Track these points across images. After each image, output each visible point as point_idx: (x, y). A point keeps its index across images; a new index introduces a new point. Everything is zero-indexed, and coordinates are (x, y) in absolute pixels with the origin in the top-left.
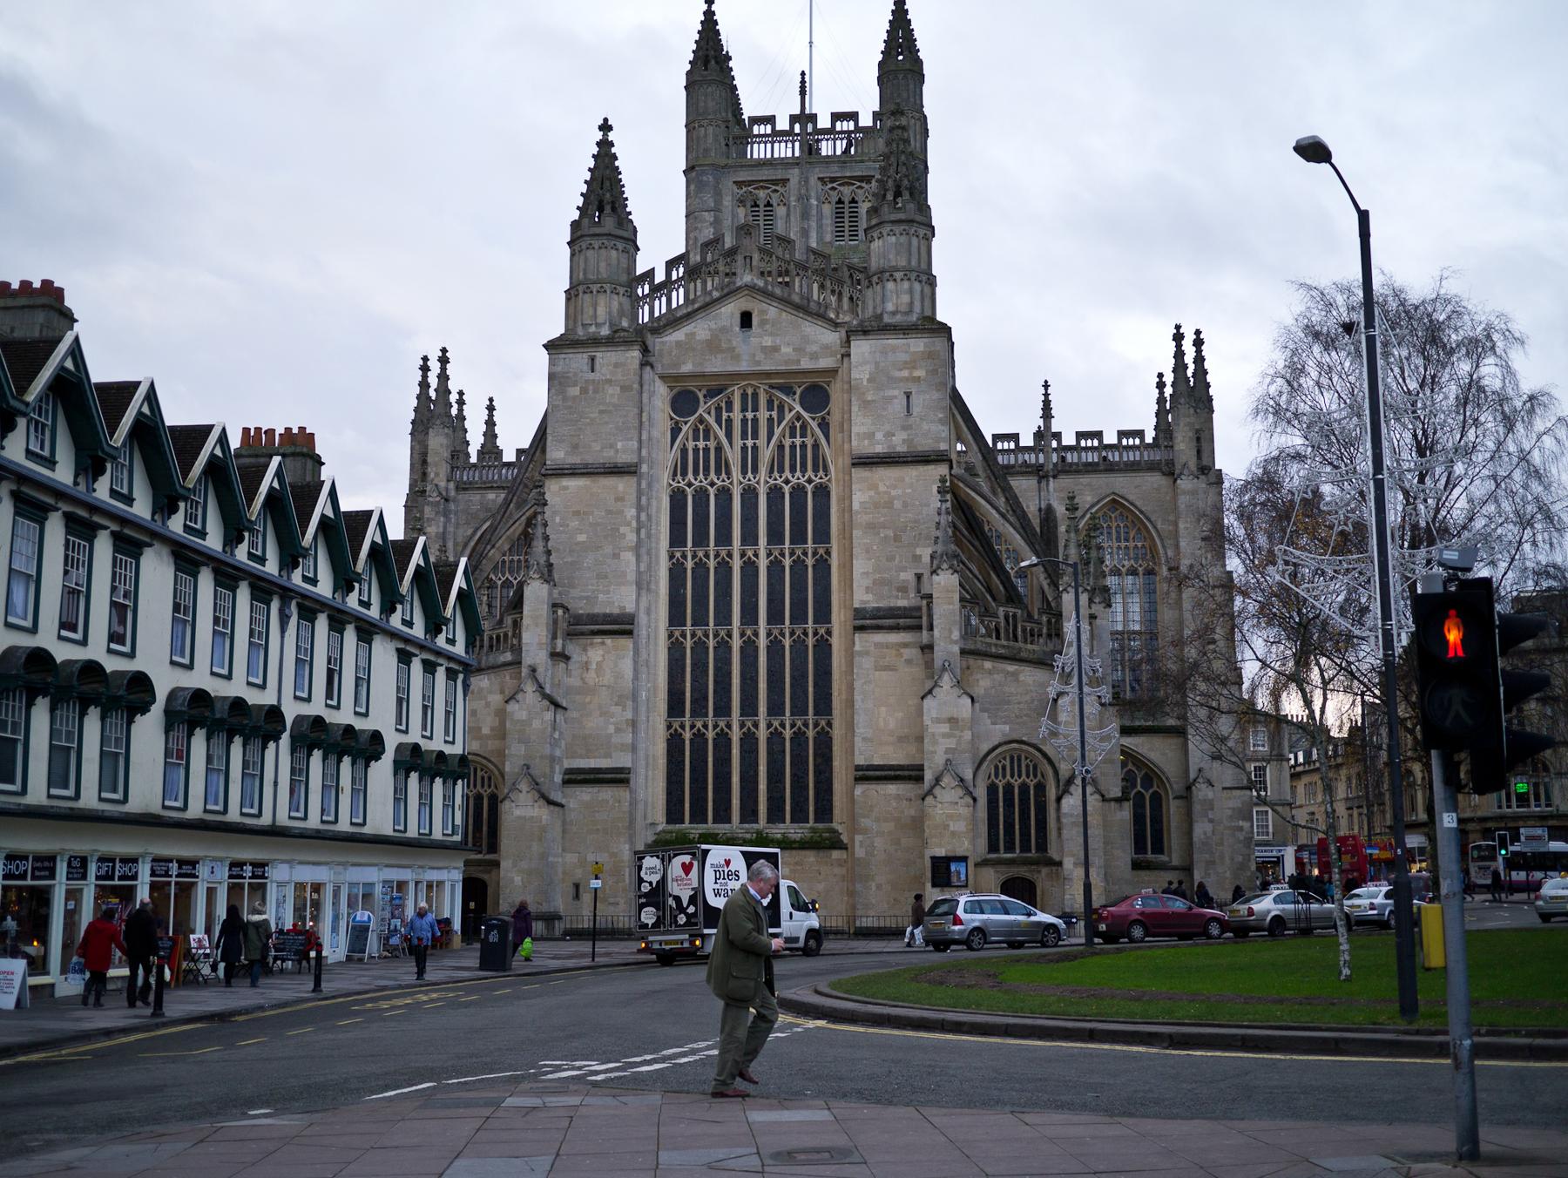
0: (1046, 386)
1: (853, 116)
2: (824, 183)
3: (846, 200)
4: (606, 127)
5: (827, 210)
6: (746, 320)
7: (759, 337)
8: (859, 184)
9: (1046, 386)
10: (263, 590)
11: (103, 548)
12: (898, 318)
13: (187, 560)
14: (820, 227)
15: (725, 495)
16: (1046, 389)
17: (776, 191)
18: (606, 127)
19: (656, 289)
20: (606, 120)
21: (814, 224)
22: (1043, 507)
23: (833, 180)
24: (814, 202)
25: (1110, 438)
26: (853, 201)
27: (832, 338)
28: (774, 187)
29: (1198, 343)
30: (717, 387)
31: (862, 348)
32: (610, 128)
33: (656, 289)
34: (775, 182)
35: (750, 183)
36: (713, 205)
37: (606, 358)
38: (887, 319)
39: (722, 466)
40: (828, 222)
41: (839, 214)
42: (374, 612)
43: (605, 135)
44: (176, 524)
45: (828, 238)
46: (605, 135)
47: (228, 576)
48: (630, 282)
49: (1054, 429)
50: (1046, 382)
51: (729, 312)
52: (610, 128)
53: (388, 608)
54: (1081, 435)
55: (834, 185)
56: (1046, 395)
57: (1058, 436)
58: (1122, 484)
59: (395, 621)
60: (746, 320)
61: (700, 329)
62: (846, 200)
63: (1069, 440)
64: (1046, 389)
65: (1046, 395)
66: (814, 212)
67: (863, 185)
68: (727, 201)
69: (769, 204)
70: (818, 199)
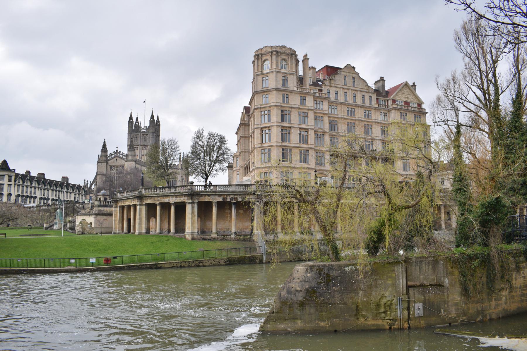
6: (117, 159)
7: (118, 161)
10: (59, 191)
11: (46, 190)
13: (52, 190)
15: (115, 176)
19: (109, 156)
27: (124, 161)
30: (114, 166)
31: (126, 163)
33: (109, 156)
37: (103, 164)
39: (114, 174)
42: (72, 191)
44: (52, 188)
47: (56, 191)
48: (106, 156)
51: (115, 159)
53: (73, 190)
59: (74, 191)
60: (117, 159)
61: (112, 161)
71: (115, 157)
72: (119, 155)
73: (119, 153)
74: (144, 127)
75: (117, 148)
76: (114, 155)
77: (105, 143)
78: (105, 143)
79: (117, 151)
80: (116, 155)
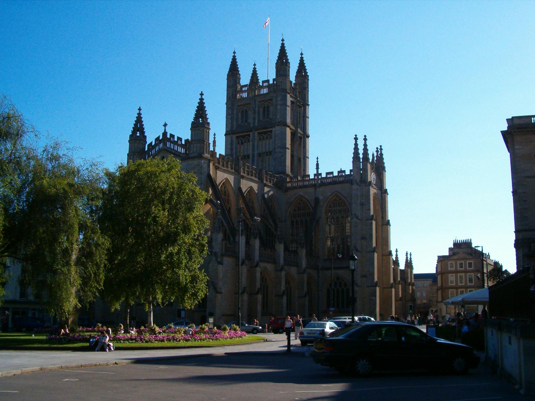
0: (317, 159)
1: (268, 81)
2: (260, 102)
3: (266, 106)
4: (140, 109)
5: (261, 110)
8: (269, 101)
9: (317, 159)
12: (193, 155)
14: (259, 115)
16: (317, 160)
17: (248, 107)
18: (140, 109)
20: (140, 107)
21: (257, 115)
22: (316, 197)
23: (262, 101)
24: (257, 109)
25: (336, 174)
26: (268, 107)
28: (247, 106)
29: (365, 139)
32: (141, 110)
34: (248, 104)
35: (241, 105)
36: (230, 113)
38: (190, 156)
40: (261, 114)
41: (264, 111)
43: (140, 111)
45: (261, 119)
46: (140, 111)
49: (319, 173)
50: (317, 157)
52: (141, 110)
54: (327, 174)
55: (263, 103)
56: (317, 161)
57: (321, 174)
58: (338, 187)
62: (266, 106)
63: (324, 175)
64: (317, 160)
65: (317, 161)
66: (257, 112)
67: (270, 101)
68: (235, 112)
69: (246, 111)
70: (258, 108)
71: (160, 151)
72: (168, 144)
73: (169, 140)
74: (263, 82)
75: (165, 125)
76: (157, 148)
77: (139, 120)
78: (139, 120)
79: (165, 134)
80: (161, 145)
